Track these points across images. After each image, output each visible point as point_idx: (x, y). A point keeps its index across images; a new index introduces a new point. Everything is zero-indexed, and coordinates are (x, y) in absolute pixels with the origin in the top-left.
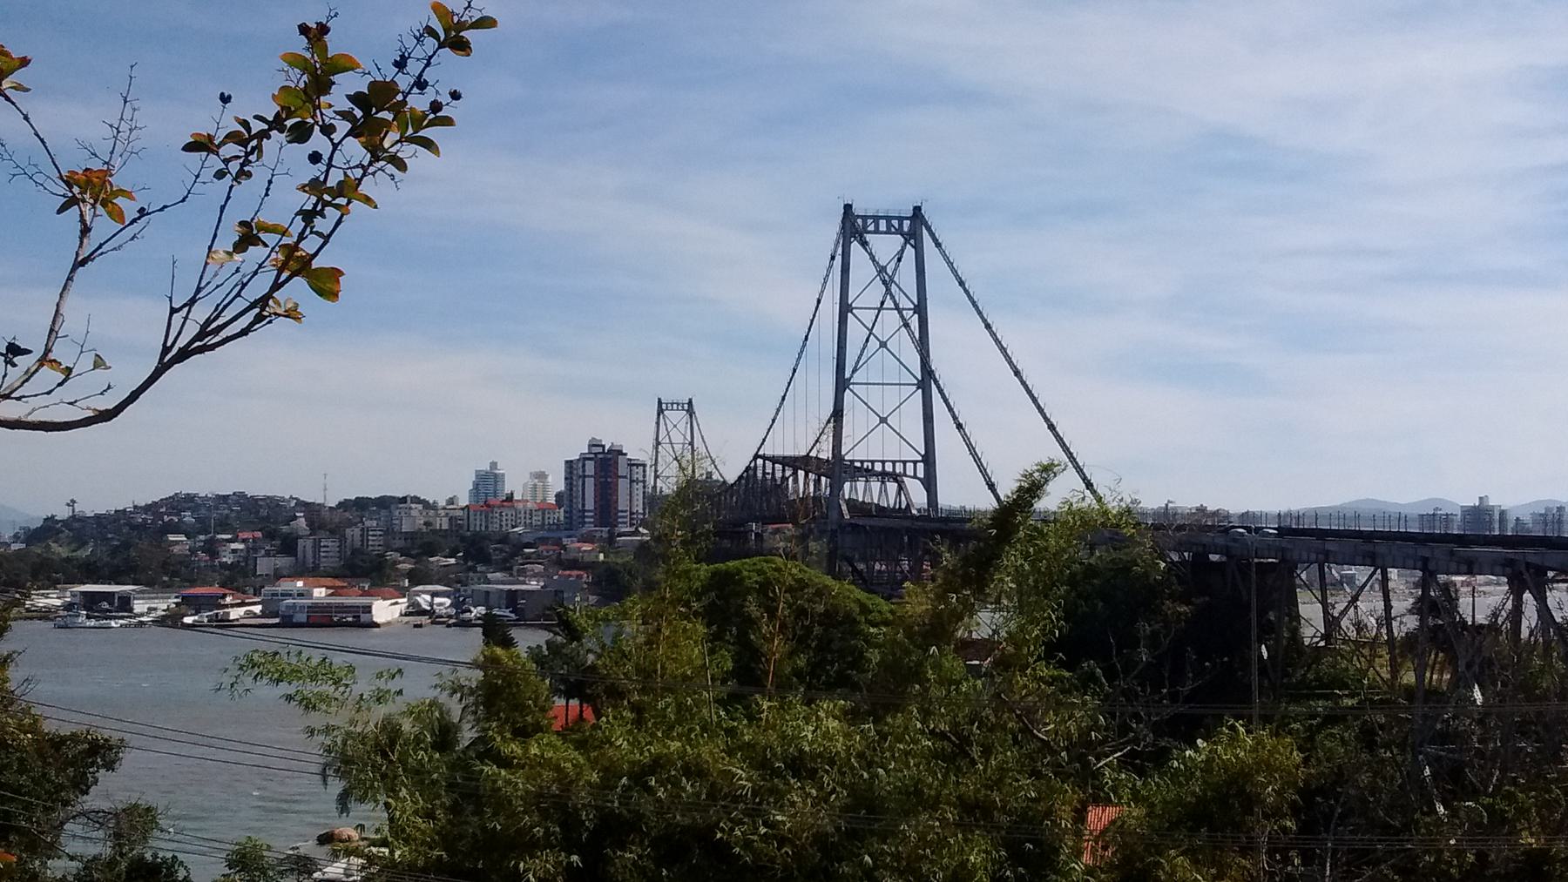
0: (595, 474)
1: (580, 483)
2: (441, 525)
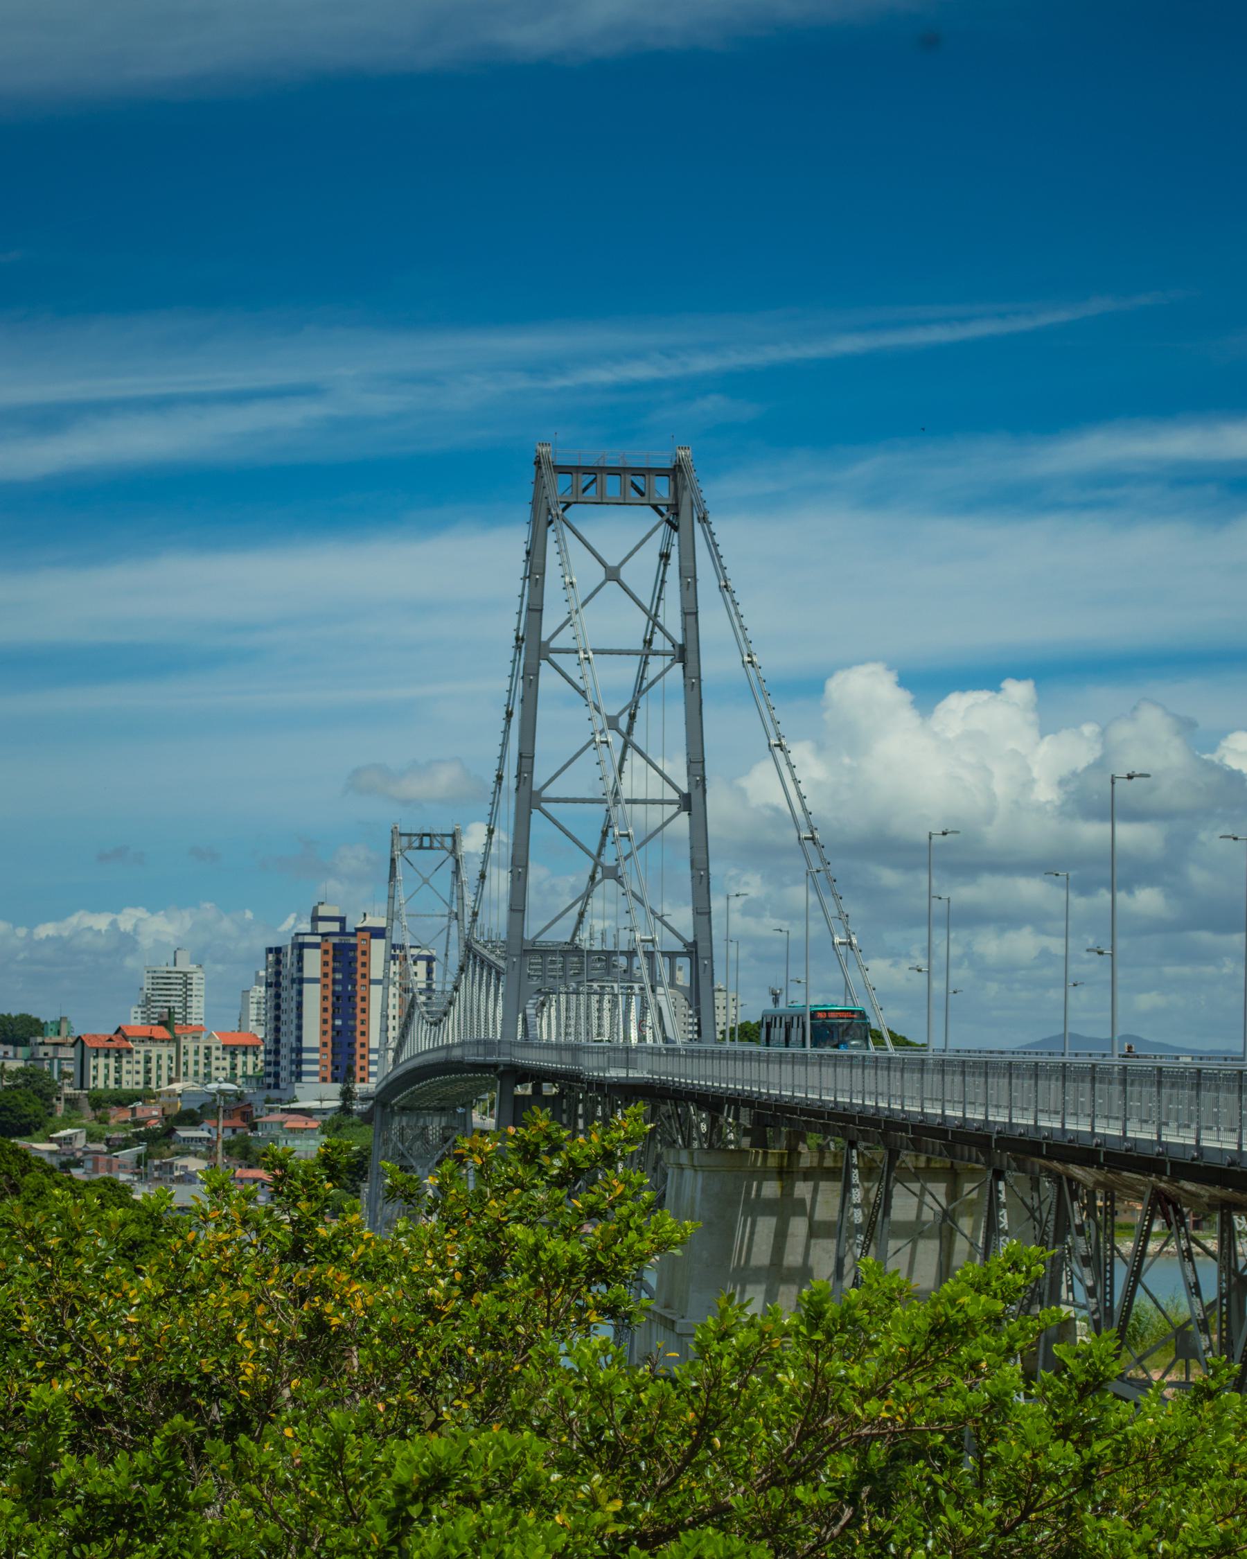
0: (325, 975)
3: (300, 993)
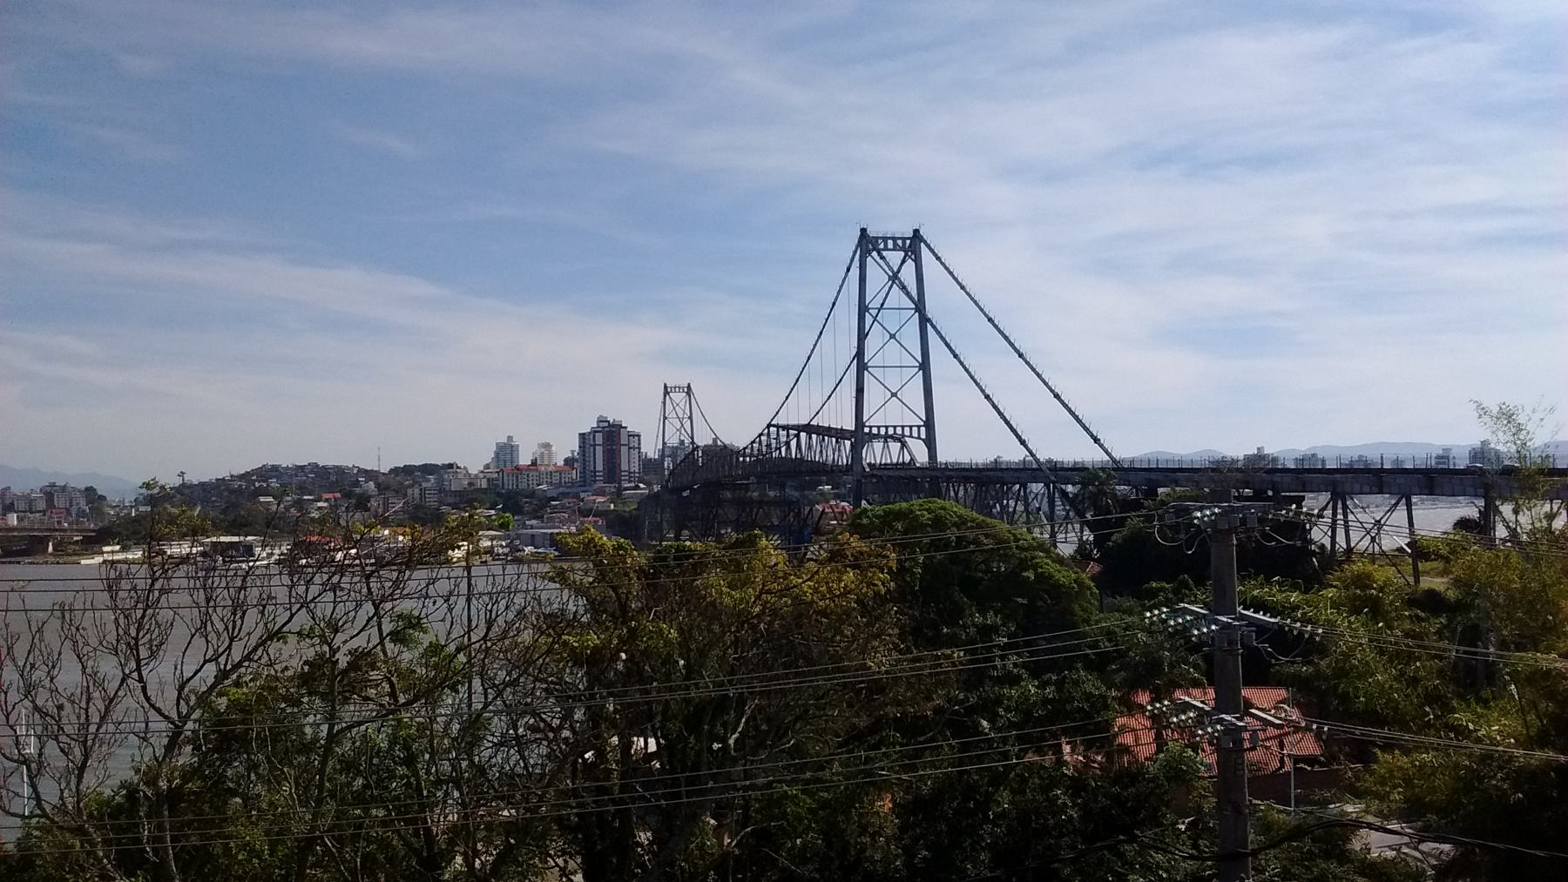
1: (592, 450)
2: (481, 485)
3: (595, 449)
